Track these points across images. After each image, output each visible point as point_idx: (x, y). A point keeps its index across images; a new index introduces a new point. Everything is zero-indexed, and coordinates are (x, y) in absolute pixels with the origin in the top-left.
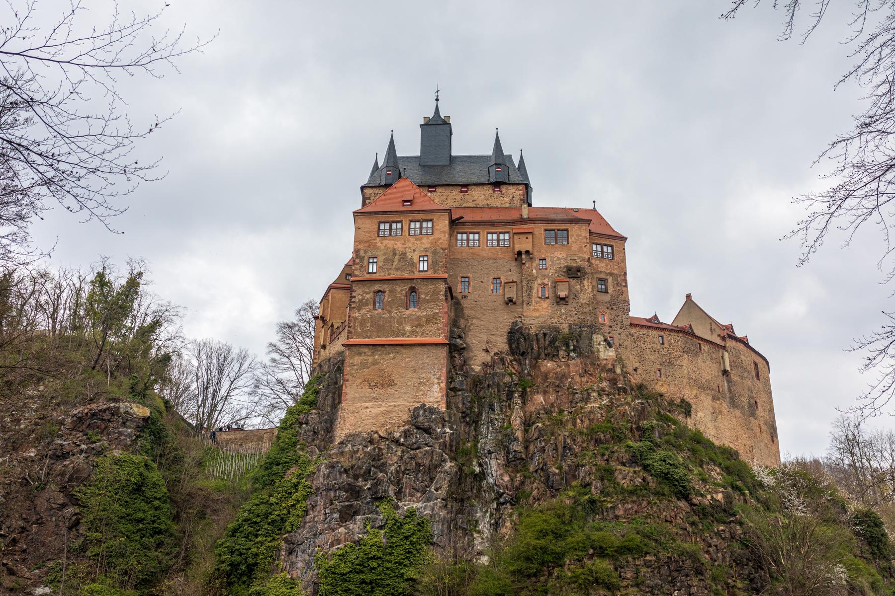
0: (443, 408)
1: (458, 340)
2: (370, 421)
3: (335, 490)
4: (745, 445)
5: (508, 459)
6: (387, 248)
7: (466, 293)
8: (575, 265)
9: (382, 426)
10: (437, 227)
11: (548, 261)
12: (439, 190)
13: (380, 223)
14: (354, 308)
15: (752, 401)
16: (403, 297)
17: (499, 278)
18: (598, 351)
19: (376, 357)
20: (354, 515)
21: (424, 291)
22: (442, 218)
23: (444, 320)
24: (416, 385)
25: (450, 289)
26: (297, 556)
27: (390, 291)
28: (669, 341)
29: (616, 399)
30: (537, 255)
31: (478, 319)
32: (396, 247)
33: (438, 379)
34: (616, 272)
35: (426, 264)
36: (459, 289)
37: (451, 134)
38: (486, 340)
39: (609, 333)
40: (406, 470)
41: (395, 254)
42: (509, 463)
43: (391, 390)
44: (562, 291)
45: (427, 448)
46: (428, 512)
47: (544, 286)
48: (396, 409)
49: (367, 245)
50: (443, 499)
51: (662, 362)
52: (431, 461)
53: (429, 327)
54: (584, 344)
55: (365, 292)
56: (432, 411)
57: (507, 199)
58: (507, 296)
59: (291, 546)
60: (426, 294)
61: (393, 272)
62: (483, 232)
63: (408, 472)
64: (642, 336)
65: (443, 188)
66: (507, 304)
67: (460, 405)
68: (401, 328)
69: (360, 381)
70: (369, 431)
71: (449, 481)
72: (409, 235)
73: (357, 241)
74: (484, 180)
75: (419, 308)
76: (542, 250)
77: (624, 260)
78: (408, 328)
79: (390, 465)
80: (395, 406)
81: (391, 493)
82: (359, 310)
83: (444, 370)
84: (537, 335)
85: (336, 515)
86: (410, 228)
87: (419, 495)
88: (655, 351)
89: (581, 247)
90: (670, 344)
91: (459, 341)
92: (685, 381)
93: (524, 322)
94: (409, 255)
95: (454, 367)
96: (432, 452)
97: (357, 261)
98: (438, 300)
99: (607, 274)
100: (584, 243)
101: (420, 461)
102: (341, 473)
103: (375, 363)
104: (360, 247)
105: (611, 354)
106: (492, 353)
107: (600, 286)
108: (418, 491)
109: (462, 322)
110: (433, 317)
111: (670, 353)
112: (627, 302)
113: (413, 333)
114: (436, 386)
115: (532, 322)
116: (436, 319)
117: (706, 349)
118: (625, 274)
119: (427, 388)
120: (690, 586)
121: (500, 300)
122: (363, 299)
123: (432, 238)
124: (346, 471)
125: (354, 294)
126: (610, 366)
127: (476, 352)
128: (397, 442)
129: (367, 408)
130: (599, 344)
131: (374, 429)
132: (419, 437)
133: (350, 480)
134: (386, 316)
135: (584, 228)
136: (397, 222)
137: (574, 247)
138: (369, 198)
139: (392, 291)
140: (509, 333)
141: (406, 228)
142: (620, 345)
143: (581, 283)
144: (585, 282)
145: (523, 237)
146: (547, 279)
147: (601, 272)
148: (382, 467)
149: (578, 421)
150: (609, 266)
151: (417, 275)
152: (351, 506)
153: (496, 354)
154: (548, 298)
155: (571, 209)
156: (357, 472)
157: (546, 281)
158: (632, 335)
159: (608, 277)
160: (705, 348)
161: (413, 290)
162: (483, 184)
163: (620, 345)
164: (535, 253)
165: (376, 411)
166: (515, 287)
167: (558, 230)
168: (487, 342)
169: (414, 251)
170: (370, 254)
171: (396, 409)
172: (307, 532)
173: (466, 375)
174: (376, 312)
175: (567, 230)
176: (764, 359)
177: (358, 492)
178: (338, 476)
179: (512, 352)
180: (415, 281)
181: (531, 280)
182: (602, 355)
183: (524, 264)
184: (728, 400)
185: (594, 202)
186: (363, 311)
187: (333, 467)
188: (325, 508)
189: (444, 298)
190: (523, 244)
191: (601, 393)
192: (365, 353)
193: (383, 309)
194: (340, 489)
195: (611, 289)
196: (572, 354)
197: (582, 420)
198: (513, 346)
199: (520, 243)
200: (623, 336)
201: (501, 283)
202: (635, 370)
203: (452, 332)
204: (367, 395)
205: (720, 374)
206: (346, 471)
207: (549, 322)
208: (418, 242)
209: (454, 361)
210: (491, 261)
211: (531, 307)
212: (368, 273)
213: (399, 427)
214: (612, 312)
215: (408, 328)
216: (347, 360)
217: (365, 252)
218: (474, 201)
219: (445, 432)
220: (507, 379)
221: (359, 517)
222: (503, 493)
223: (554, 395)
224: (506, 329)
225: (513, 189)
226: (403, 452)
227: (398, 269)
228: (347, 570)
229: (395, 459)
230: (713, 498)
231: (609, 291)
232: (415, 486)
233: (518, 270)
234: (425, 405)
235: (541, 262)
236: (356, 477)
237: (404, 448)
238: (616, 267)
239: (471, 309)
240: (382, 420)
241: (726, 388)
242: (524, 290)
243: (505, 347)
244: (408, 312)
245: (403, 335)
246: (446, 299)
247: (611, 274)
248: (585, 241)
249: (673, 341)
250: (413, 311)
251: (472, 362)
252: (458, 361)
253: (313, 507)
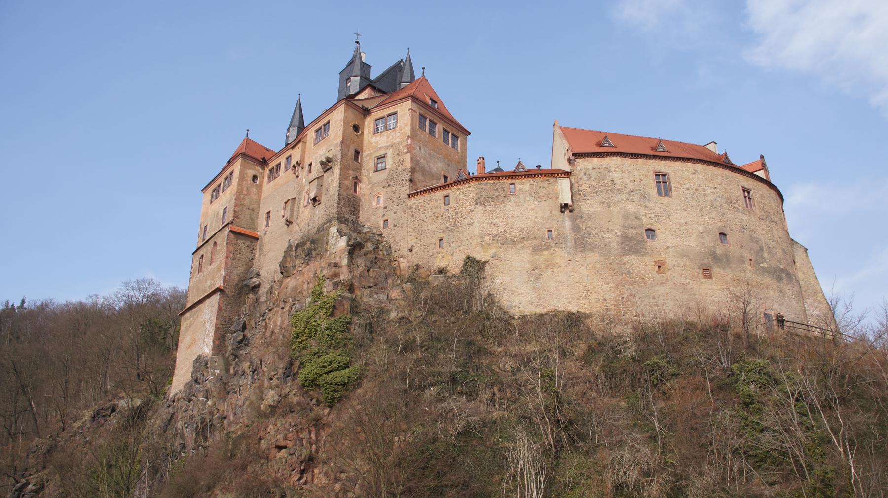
4: (605, 300)
51: (445, 228)
64: (423, 204)
88: (437, 217)
92: (474, 242)
99: (387, 148)
142: (395, 226)
147: (380, 148)
150: (391, 137)
184: (570, 244)
205: (557, 212)
231: (388, 167)
247: (392, 146)
249: (462, 196)
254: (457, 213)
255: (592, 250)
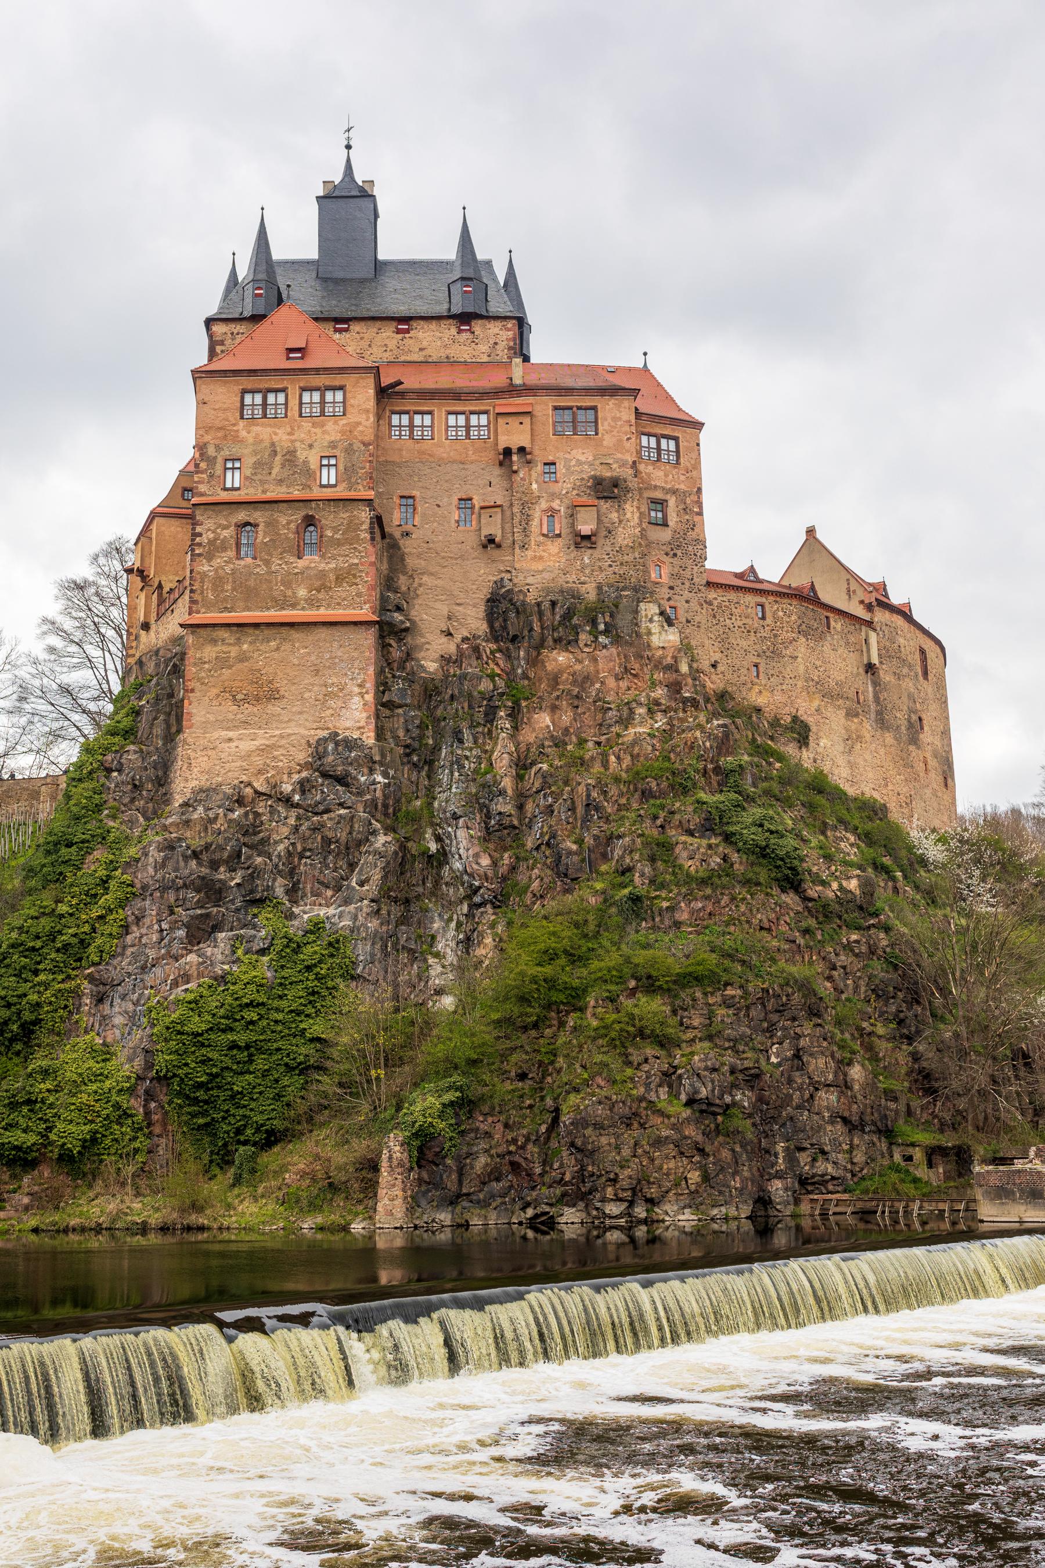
0: (369, 738)
1: (396, 615)
2: (238, 764)
3: (178, 889)
5: (487, 828)
6: (258, 441)
7: (409, 527)
8: (609, 474)
9: (260, 772)
10: (352, 401)
11: (560, 467)
12: (355, 327)
13: (244, 392)
14: (199, 555)
15: (914, 717)
16: (291, 536)
17: (470, 499)
18: (649, 633)
19: (245, 647)
20: (213, 932)
21: (331, 521)
22: (363, 383)
23: (368, 578)
24: (320, 697)
25: (379, 520)
26: (112, 1006)
27: (268, 524)
28: (774, 613)
29: (679, 719)
30: (540, 456)
31: (432, 574)
32: (275, 438)
33: (360, 686)
34: (682, 487)
35: (333, 471)
36: (395, 519)
37: (376, 216)
38: (446, 613)
39: (669, 599)
40: (304, 850)
41: (275, 453)
42: (489, 834)
43: (273, 708)
44: (585, 523)
45: (342, 811)
46: (347, 922)
47: (552, 513)
48: (283, 742)
49: (220, 434)
50: (372, 901)
52: (350, 833)
53: (342, 591)
54: (623, 621)
55: (219, 526)
56: (349, 744)
57: (484, 348)
58: (485, 532)
59: (101, 988)
60: (335, 530)
61: (272, 487)
62: (440, 410)
63: (308, 854)
65: (363, 324)
66: (485, 547)
67: (401, 733)
68: (289, 593)
69: (215, 691)
70: (236, 782)
71: (384, 868)
72: (301, 415)
73: (202, 427)
74: (442, 309)
75: (323, 556)
76: (547, 448)
77: (697, 465)
78: (302, 593)
79: (276, 842)
80: (282, 737)
81: (279, 891)
82: (209, 560)
83: (371, 670)
84: (539, 604)
85: (181, 933)
86: (301, 403)
87: (329, 893)
89: (621, 441)
90: (776, 619)
91: (398, 617)
92: (800, 684)
93: (515, 581)
94: (302, 455)
95: (389, 664)
96: (352, 817)
97: (203, 465)
98: (357, 539)
100: (626, 433)
101: (330, 834)
102: (186, 858)
103: (243, 658)
104: (207, 438)
105: (671, 637)
106: (458, 638)
107: (653, 514)
108: (328, 887)
109: (402, 581)
110: (348, 573)
111: (775, 636)
112: (701, 542)
113: (312, 603)
114: (356, 699)
115: (530, 580)
116: (354, 576)
117: (839, 626)
118: (699, 490)
119: (340, 704)
120: (798, 1036)
121: (472, 541)
122: (215, 539)
123: (344, 422)
124: (196, 855)
125: (198, 529)
126: (669, 660)
127: (430, 637)
128: (287, 801)
129: (230, 740)
130: (651, 621)
131: (244, 778)
132: (327, 792)
133: (205, 871)
134: (262, 570)
135: (626, 404)
136: (276, 391)
137: (608, 441)
138: (222, 343)
139: (271, 524)
140: (488, 601)
141: (294, 403)
142: (688, 621)
143: (620, 509)
144: (627, 506)
145: (514, 421)
146: (558, 502)
147: (656, 487)
148: (262, 846)
149: (613, 758)
151: (316, 493)
152: (207, 916)
153: (465, 639)
154: (559, 536)
155: (603, 368)
156: (217, 856)
157: (556, 504)
158: (710, 603)
159: (668, 497)
160: (837, 624)
161: (309, 521)
162: (439, 318)
163: (688, 621)
164: (536, 452)
165: (246, 746)
166: (499, 516)
167: (579, 408)
168: (449, 618)
169: (311, 446)
170: (226, 453)
171: (283, 742)
172: (129, 964)
173: (411, 679)
174: (242, 563)
175: (594, 408)
176: (938, 643)
177: (220, 891)
178: (182, 864)
179: (495, 636)
180: (313, 505)
181: (528, 503)
182: (656, 640)
183: (516, 472)
184: (873, 716)
185: (645, 354)
186: (217, 562)
187: (172, 848)
188: (159, 921)
189: (368, 536)
190: (515, 436)
191: (653, 708)
192: (223, 640)
193: (255, 558)
194: (185, 886)
195: (673, 519)
196: (602, 639)
197: (618, 758)
198: (497, 625)
199: (508, 433)
200: (694, 604)
201: (472, 508)
202: (714, 666)
203: (384, 600)
204: (231, 716)
205: (862, 670)
206: (196, 855)
207: (561, 581)
208: (318, 430)
209: (389, 652)
210: (455, 467)
211: (530, 553)
212: (225, 489)
213: (290, 774)
214: (675, 561)
215: (302, 593)
216: (191, 653)
217: (218, 448)
218: (421, 349)
219: (374, 783)
220: (485, 685)
221: (221, 935)
222: (480, 888)
223: (570, 714)
224: (484, 593)
225: (494, 328)
226: (298, 818)
227: (280, 482)
228: (204, 1027)
229: (285, 831)
230: (841, 888)
231: (670, 523)
232: (322, 878)
233: (505, 484)
234: (337, 734)
235: (547, 469)
236: (214, 865)
237: (301, 811)
238: (682, 478)
239: (419, 556)
240: (258, 761)
241: (871, 695)
242: (516, 520)
243: (483, 627)
244: (301, 564)
245: (293, 606)
246: (373, 539)
247: (674, 492)
248: (627, 428)
249: (781, 614)
250: (311, 560)
251: (422, 654)
252: (396, 654)
253: (138, 920)
254: (775, 636)
255: (888, 729)
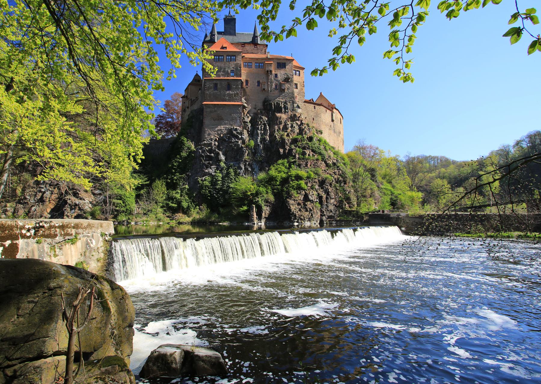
103: (215, 111)
113: (229, 101)
134: (219, 93)
136: (221, 56)
141: (225, 58)
216: (205, 110)
